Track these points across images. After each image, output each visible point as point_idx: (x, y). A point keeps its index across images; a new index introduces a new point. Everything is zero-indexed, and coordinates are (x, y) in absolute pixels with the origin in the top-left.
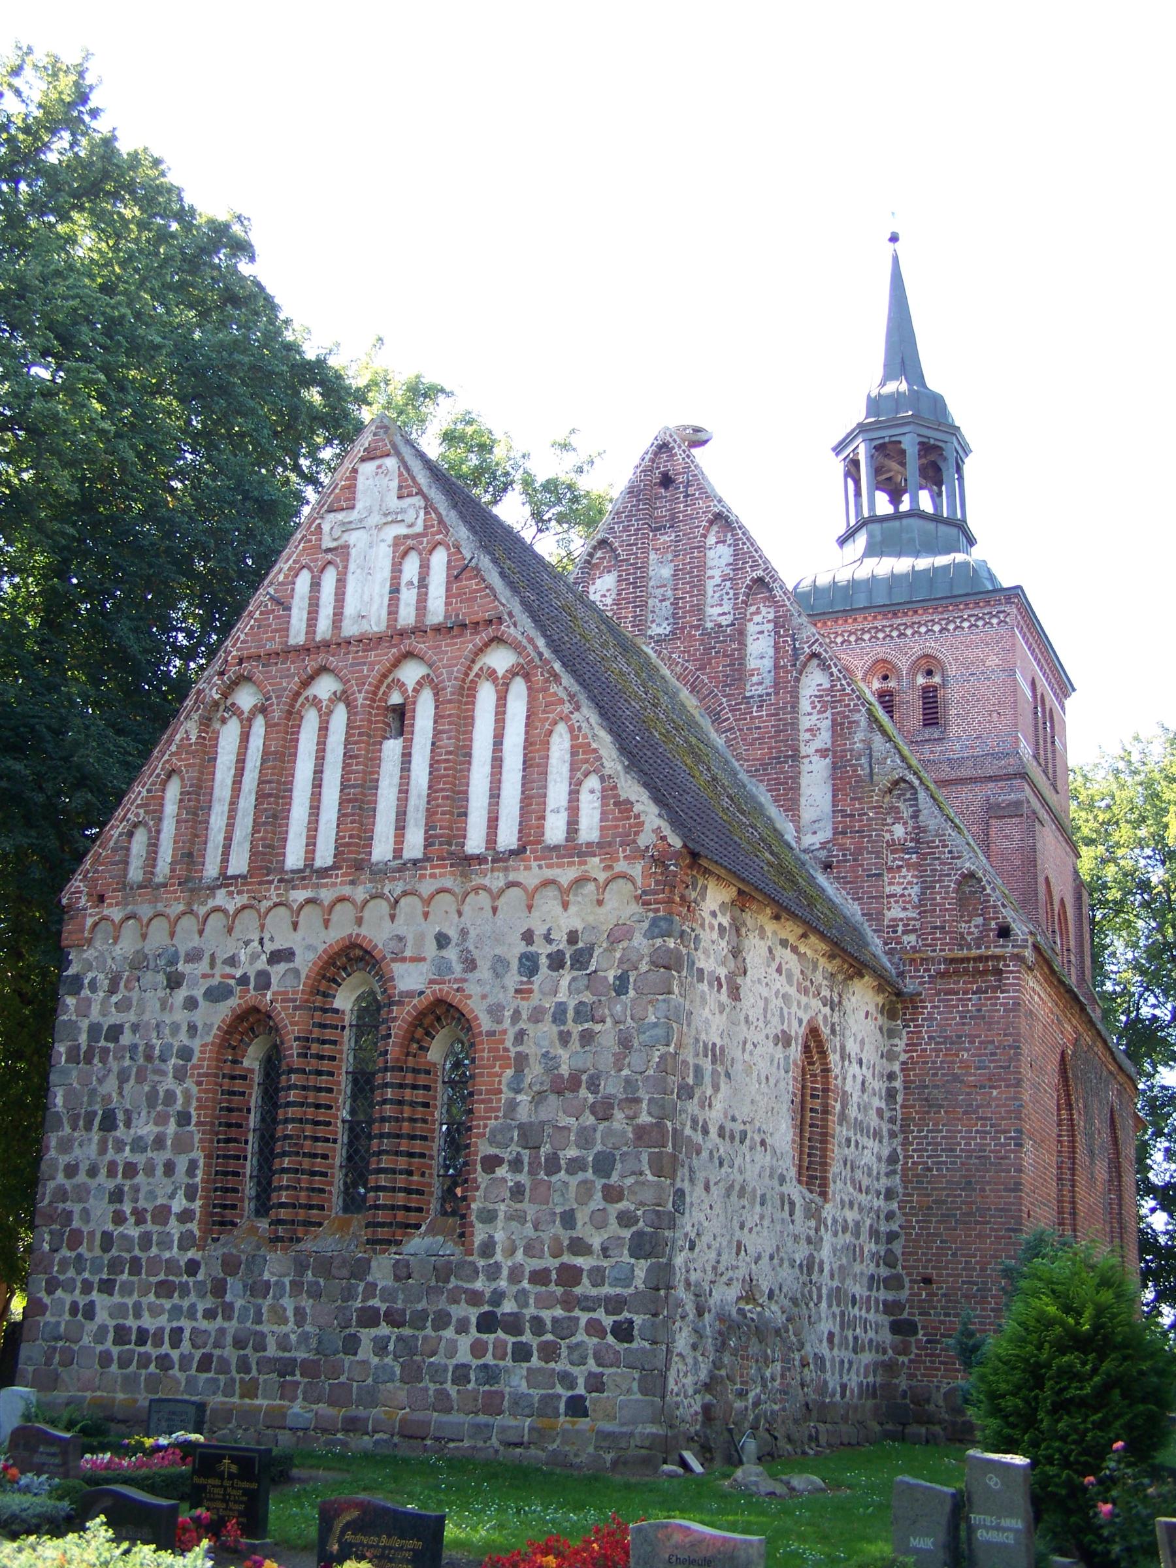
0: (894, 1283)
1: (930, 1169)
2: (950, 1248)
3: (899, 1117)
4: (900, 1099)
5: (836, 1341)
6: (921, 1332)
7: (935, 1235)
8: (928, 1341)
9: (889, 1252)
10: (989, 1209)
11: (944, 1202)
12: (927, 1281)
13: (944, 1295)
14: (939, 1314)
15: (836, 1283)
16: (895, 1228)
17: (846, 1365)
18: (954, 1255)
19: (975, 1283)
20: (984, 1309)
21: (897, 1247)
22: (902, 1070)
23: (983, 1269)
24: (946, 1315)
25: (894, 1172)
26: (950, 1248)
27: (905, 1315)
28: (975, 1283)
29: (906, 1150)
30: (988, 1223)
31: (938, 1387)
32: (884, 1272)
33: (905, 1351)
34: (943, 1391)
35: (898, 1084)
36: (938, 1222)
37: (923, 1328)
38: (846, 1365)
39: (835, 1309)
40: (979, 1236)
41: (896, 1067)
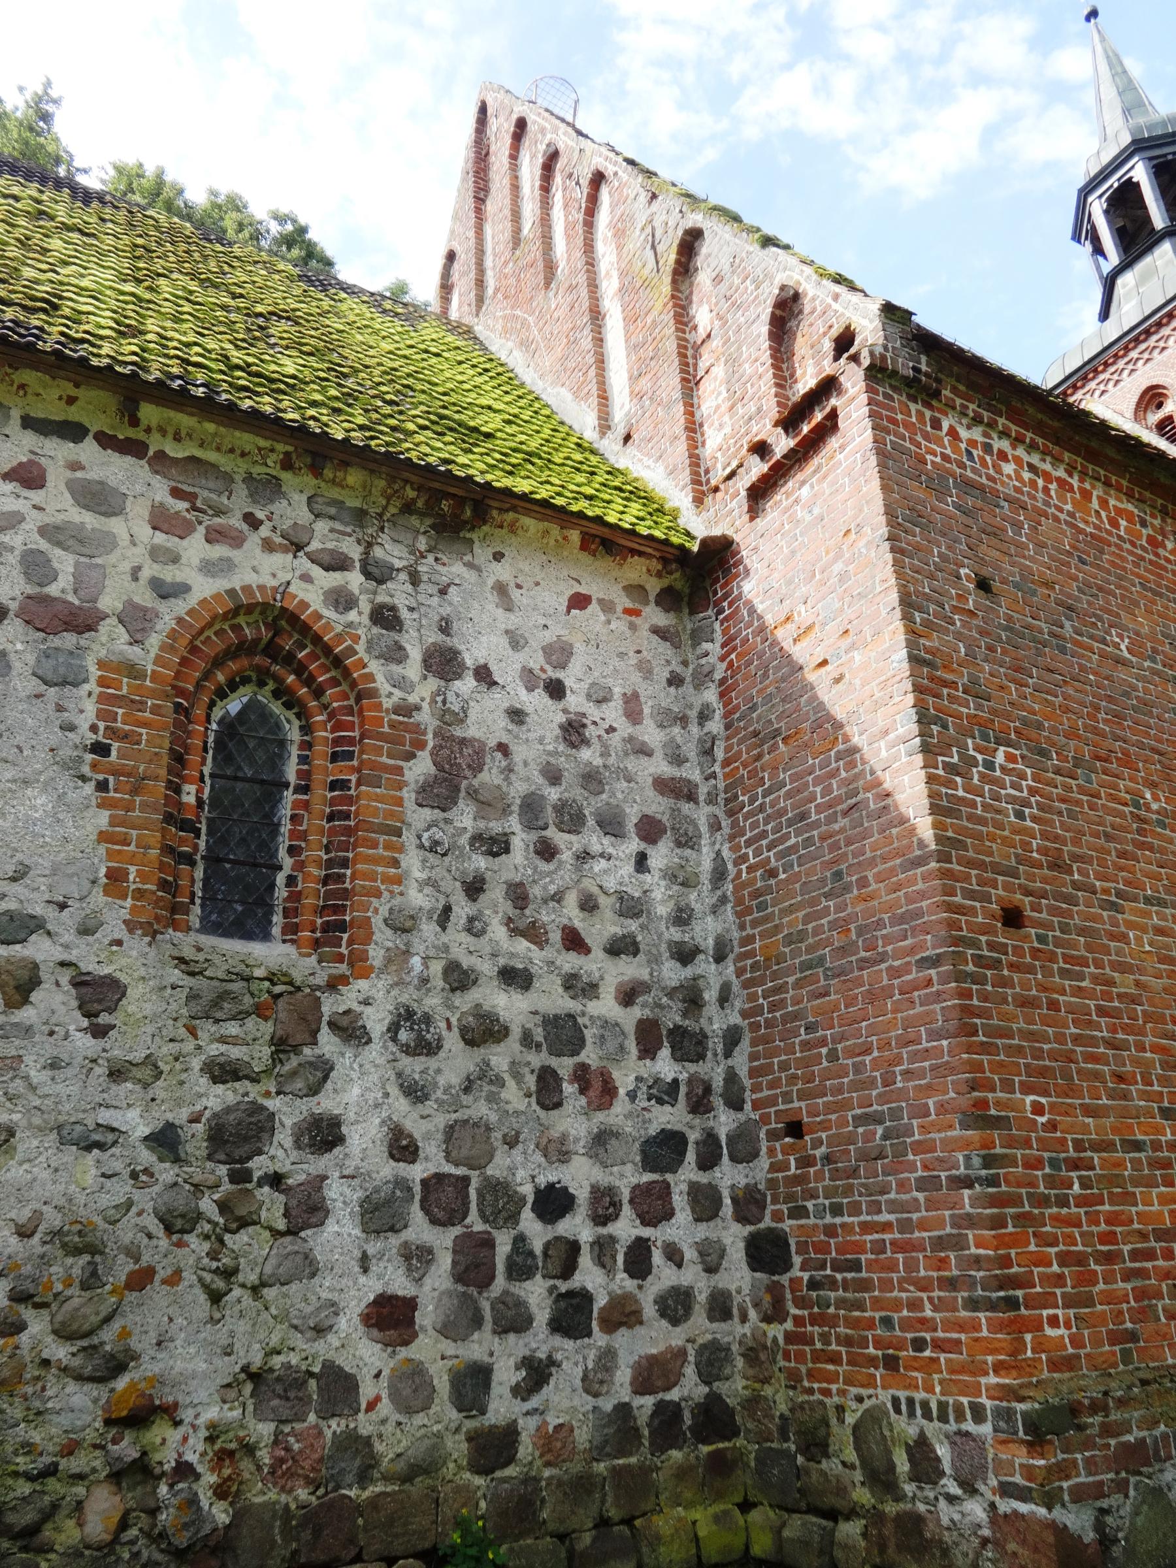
0: (744, 1149)
1: (773, 873)
2: (823, 1042)
3: (721, 785)
4: (720, 754)
5: (426, 1316)
6: (797, 1260)
7: (796, 1016)
8: (813, 1285)
9: (731, 1077)
10: (880, 924)
11: (802, 936)
12: (795, 1129)
13: (828, 1159)
14: (820, 1214)
15: (417, 1172)
16: (735, 1019)
17: (506, 1375)
18: (833, 1056)
19: (877, 1119)
20: (902, 1186)
21: (741, 1061)
22: (722, 695)
23: (888, 1081)
24: (837, 1210)
25: (723, 900)
26: (823, 1042)
27: (767, 1222)
28: (877, 1119)
29: (735, 849)
30: (883, 957)
31: (840, 1409)
32: (724, 1122)
33: (775, 1314)
34: (850, 1419)
35: (715, 725)
36: (798, 985)
37: (802, 1248)
38: (506, 1375)
39: (419, 1229)
40: (872, 997)
41: (711, 695)
